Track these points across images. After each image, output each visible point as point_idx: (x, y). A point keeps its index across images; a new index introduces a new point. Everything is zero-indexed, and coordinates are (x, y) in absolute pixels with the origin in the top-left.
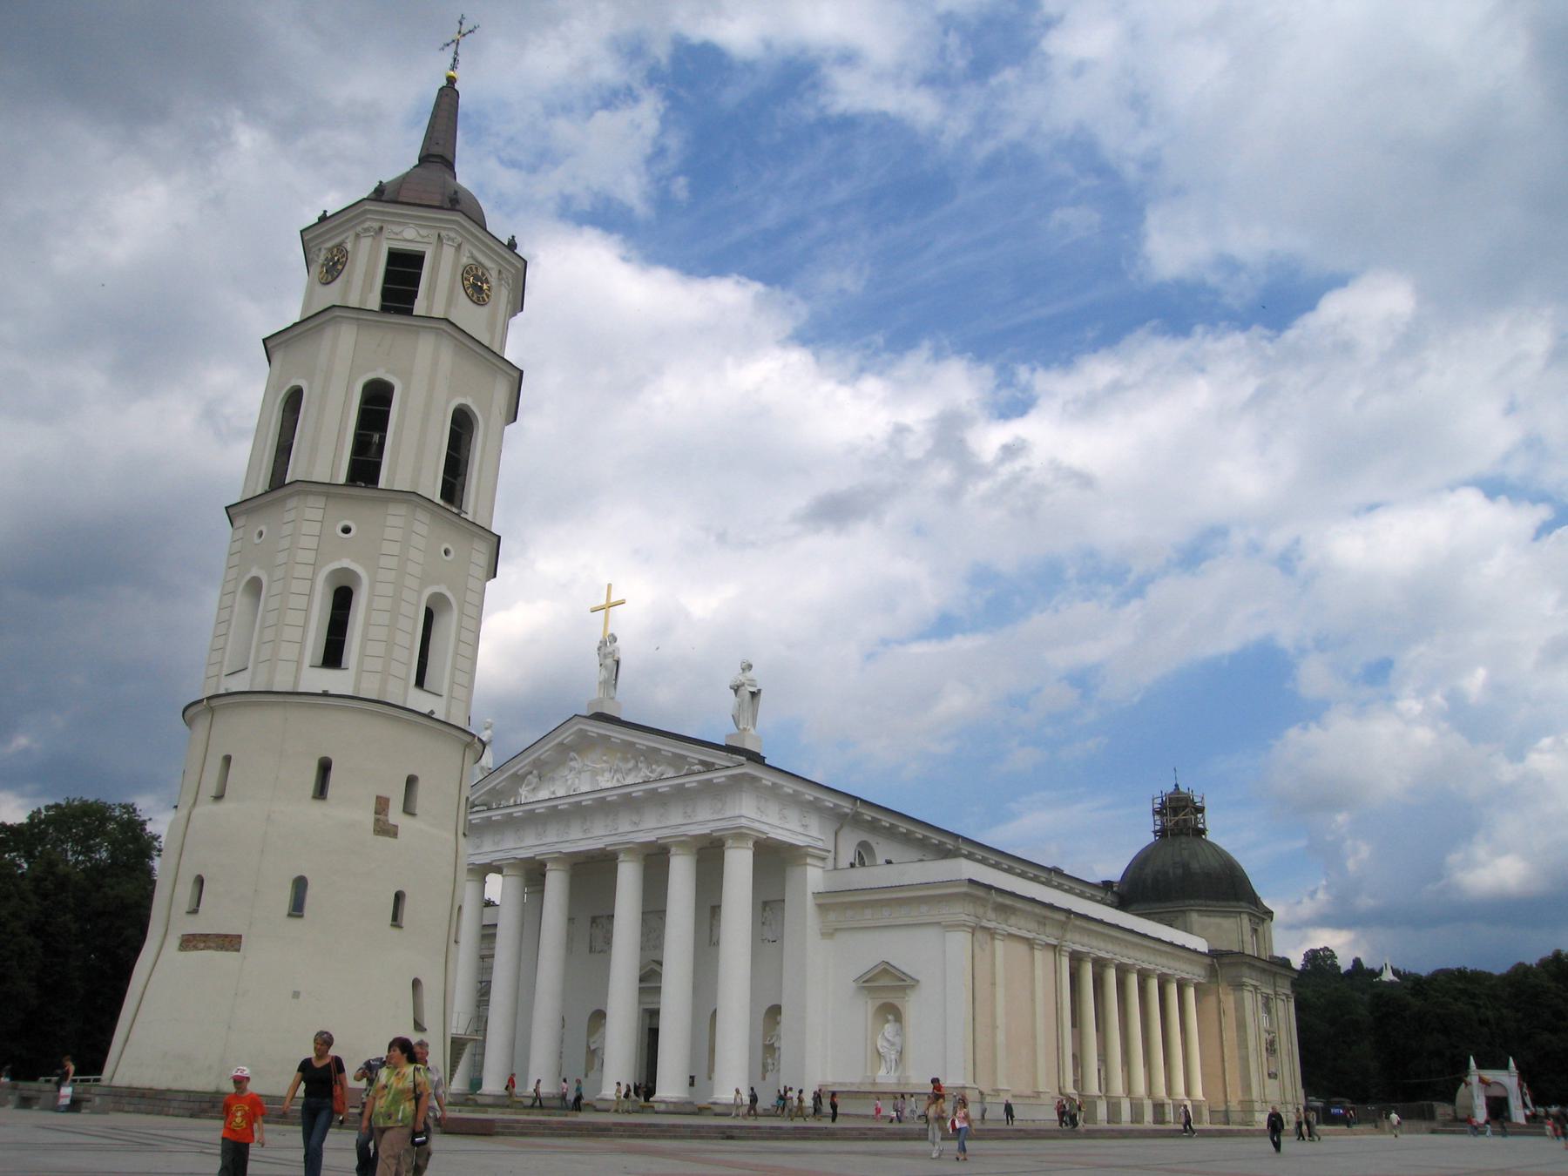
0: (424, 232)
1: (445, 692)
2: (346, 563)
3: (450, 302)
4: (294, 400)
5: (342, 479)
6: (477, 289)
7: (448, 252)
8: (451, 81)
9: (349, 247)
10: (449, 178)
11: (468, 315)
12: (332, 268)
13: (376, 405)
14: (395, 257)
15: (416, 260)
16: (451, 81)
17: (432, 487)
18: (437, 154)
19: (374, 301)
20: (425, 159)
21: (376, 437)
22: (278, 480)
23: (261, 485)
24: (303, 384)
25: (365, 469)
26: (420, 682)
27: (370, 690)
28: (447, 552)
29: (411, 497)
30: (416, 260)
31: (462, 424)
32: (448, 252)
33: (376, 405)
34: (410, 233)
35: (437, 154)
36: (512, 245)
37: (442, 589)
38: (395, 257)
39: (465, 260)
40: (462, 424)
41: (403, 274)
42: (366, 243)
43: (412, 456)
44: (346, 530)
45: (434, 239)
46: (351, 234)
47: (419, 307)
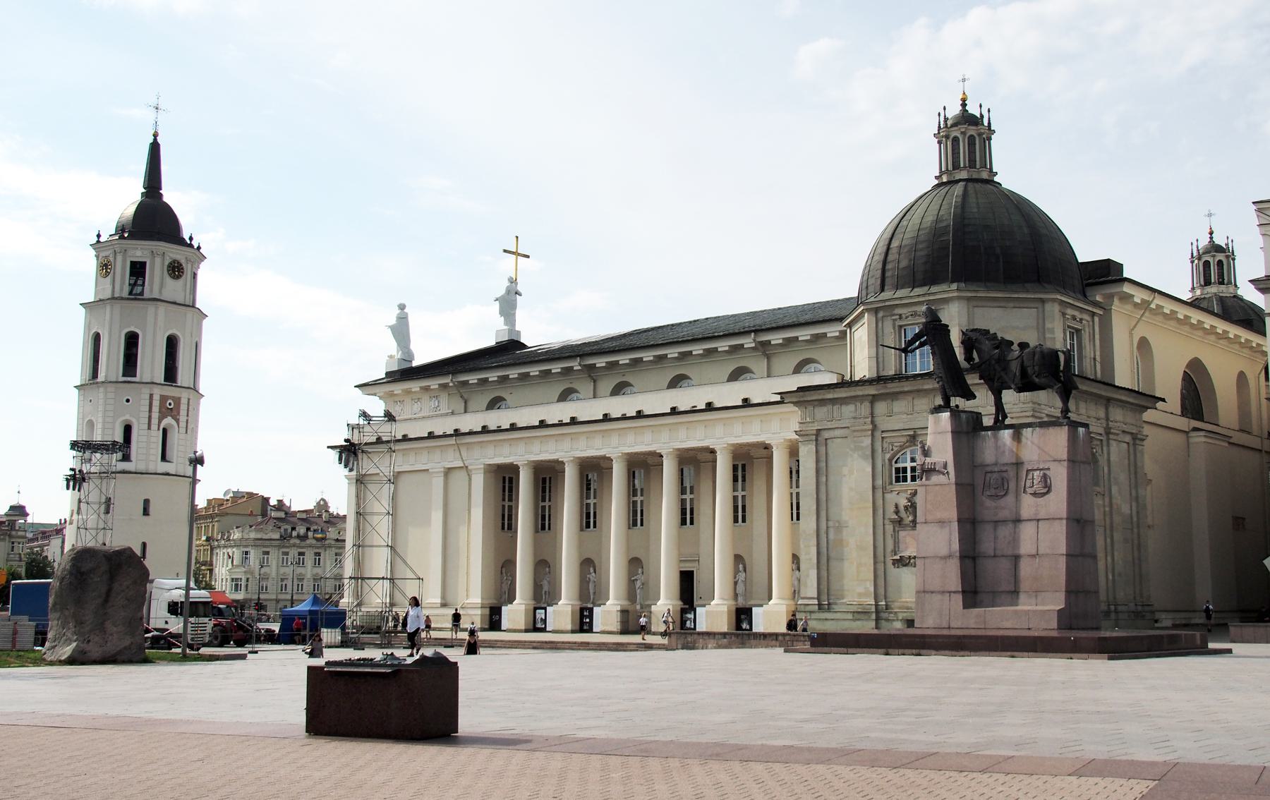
2: (127, 417)
3: (162, 285)
4: (97, 338)
6: (176, 270)
7: (158, 260)
8: (155, 139)
9: (111, 259)
12: (105, 268)
13: (132, 341)
14: (133, 264)
15: (143, 264)
16: (155, 139)
26: (164, 458)
27: (142, 467)
30: (143, 264)
31: (172, 343)
32: (158, 260)
34: (139, 253)
36: (191, 239)
38: (133, 264)
40: (172, 343)
42: (119, 258)
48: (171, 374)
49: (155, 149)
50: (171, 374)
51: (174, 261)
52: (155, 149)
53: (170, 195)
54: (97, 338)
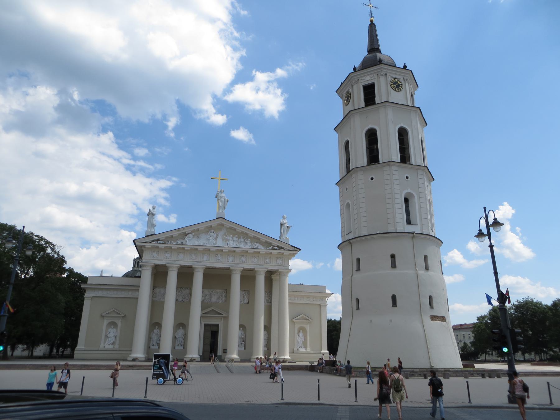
0: (371, 76)
1: (418, 223)
4: (347, 143)
5: (366, 164)
6: (397, 86)
8: (372, 21)
9: (350, 90)
10: (378, 54)
11: (396, 97)
12: (347, 99)
16: (372, 21)
17: (396, 156)
18: (374, 47)
19: (363, 104)
20: (369, 52)
21: (375, 147)
22: (348, 170)
23: (345, 173)
24: (348, 139)
25: (373, 157)
26: (409, 222)
28: (407, 178)
29: (390, 163)
32: (382, 79)
33: (372, 137)
34: (368, 78)
35: (374, 47)
36: (405, 67)
37: (409, 190)
39: (389, 79)
41: (369, 93)
42: (355, 87)
43: (389, 149)
44: (372, 179)
45: (375, 76)
46: (350, 86)
47: (377, 100)
48: (405, 158)
49: (372, 26)
50: (405, 158)
51: (395, 78)
52: (372, 26)
53: (387, 50)
54: (347, 143)
